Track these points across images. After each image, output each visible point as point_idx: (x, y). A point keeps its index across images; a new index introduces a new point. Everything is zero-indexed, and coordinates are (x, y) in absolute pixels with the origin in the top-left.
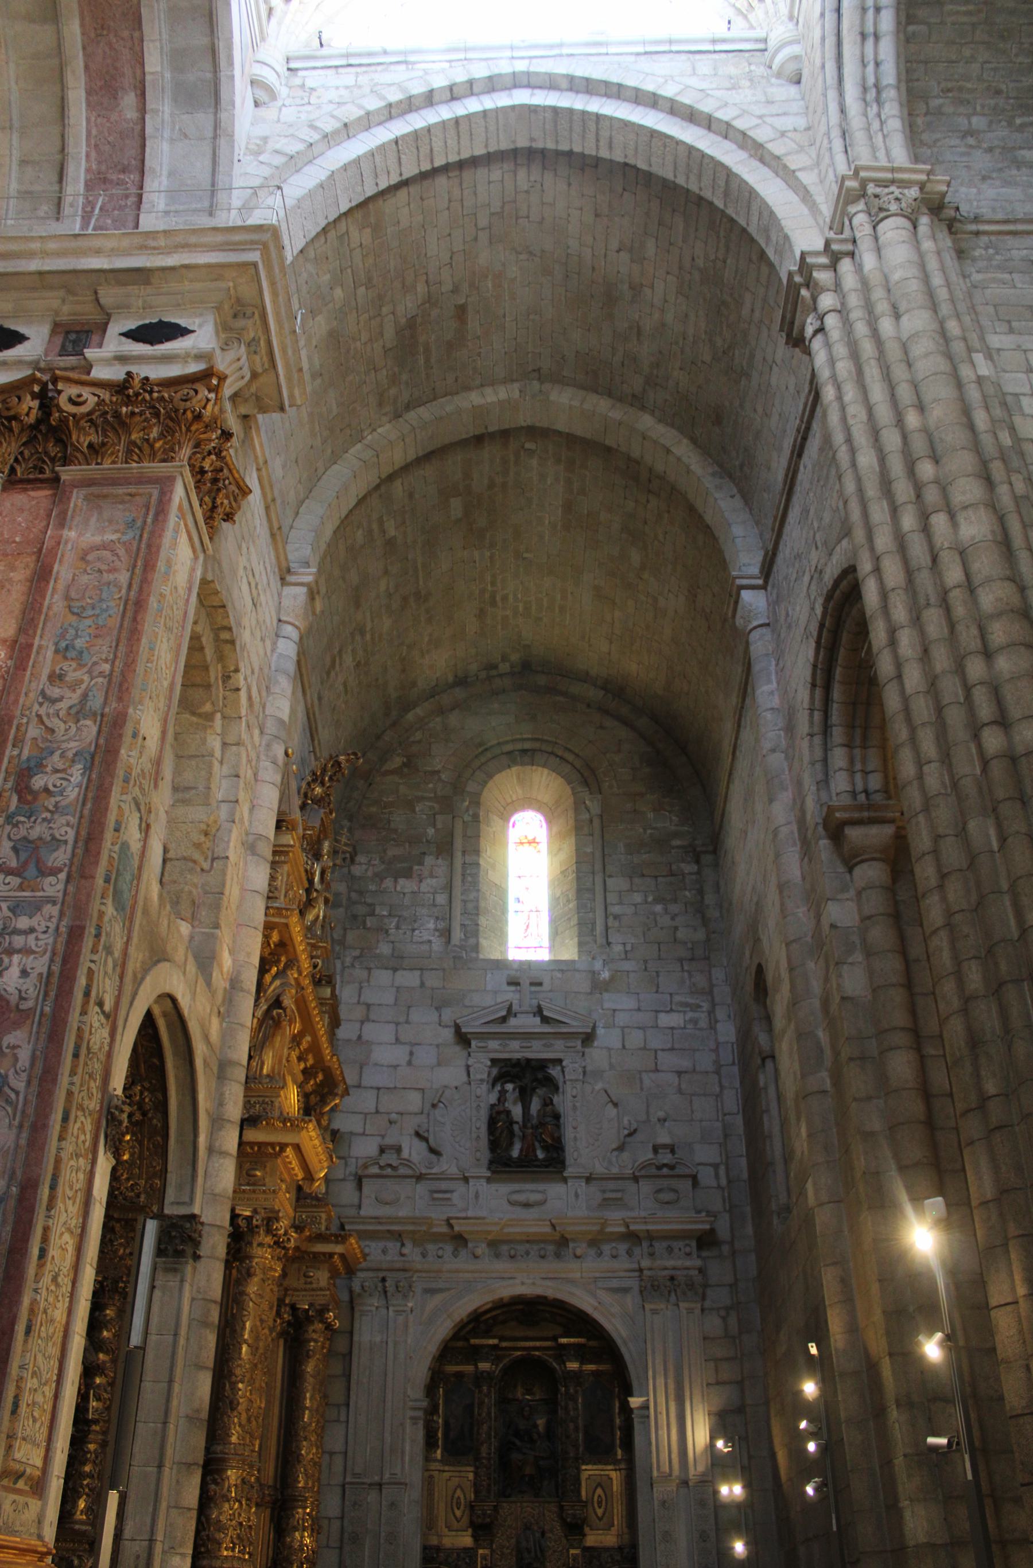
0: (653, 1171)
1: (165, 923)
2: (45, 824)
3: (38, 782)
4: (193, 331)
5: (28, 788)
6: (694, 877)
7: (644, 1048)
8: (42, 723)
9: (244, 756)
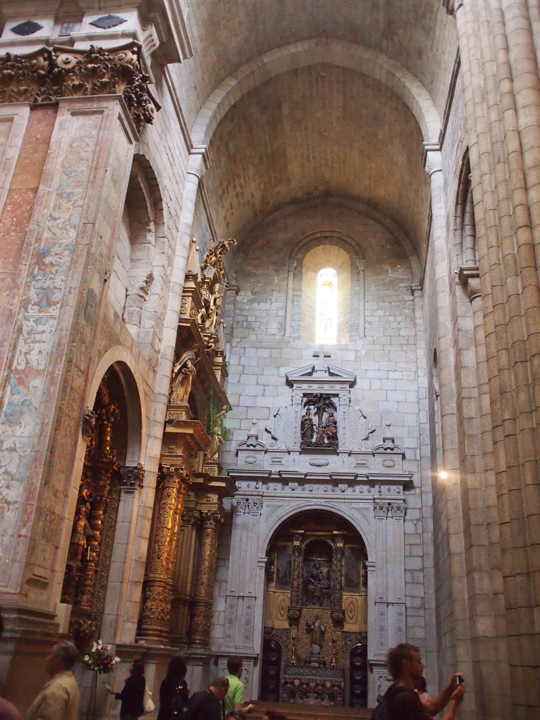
0: (382, 451)
1: (119, 328)
2: (51, 280)
3: (47, 260)
4: (126, 21)
5: (43, 263)
6: (411, 302)
7: (381, 389)
8: (50, 230)
9: (167, 243)
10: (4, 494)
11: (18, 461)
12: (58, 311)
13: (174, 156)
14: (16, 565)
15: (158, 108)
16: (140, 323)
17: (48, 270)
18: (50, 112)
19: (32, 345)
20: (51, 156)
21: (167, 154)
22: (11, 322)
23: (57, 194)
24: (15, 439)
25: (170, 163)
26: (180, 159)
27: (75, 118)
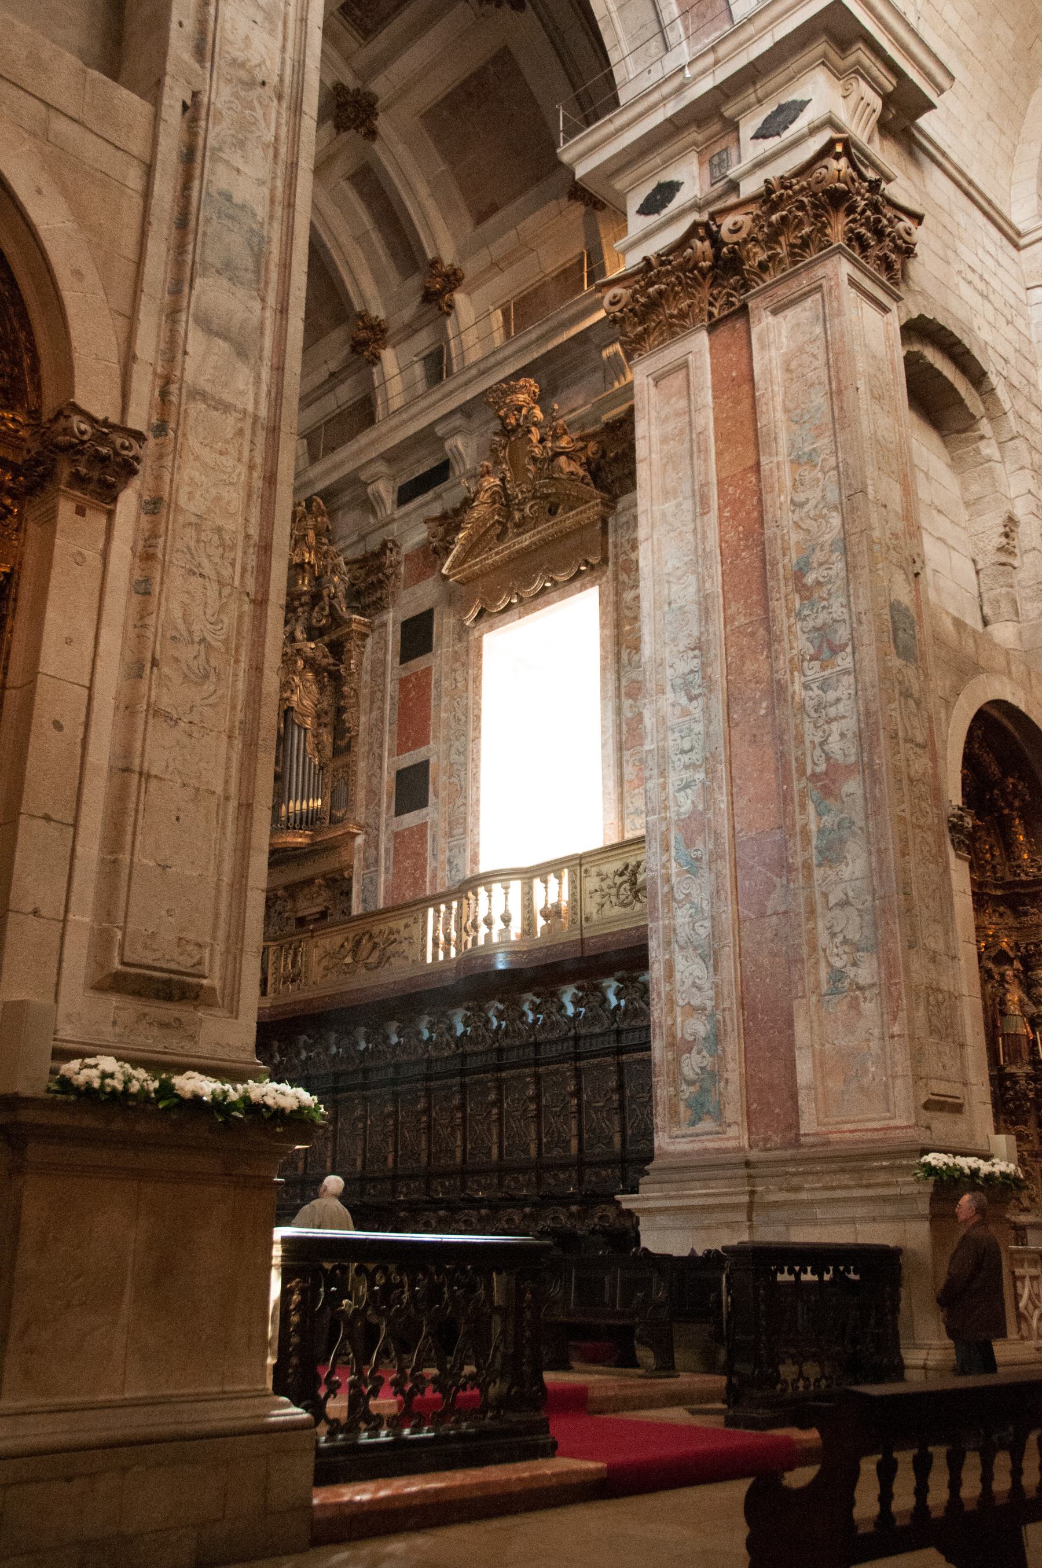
3: (810, 579)
8: (799, 527)
10: (852, 975)
11: (858, 919)
12: (850, 659)
13: (986, 276)
14: (899, 1082)
15: (918, 218)
16: (1017, 614)
17: (816, 595)
18: (739, 325)
19: (826, 727)
20: (763, 400)
21: (970, 283)
22: (786, 701)
23: (792, 462)
24: (843, 885)
25: (982, 295)
26: (1001, 273)
27: (780, 316)
